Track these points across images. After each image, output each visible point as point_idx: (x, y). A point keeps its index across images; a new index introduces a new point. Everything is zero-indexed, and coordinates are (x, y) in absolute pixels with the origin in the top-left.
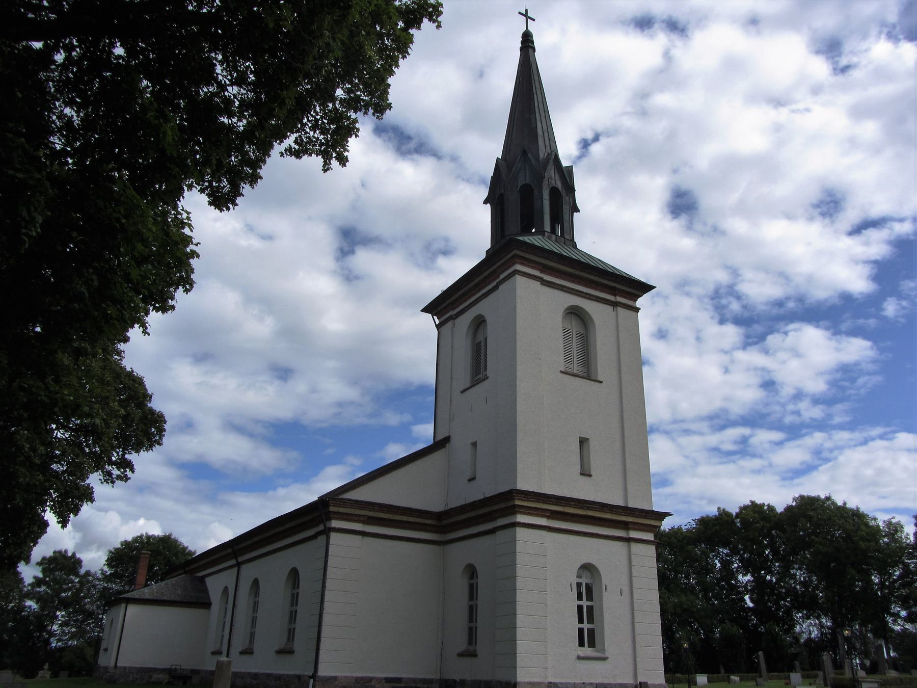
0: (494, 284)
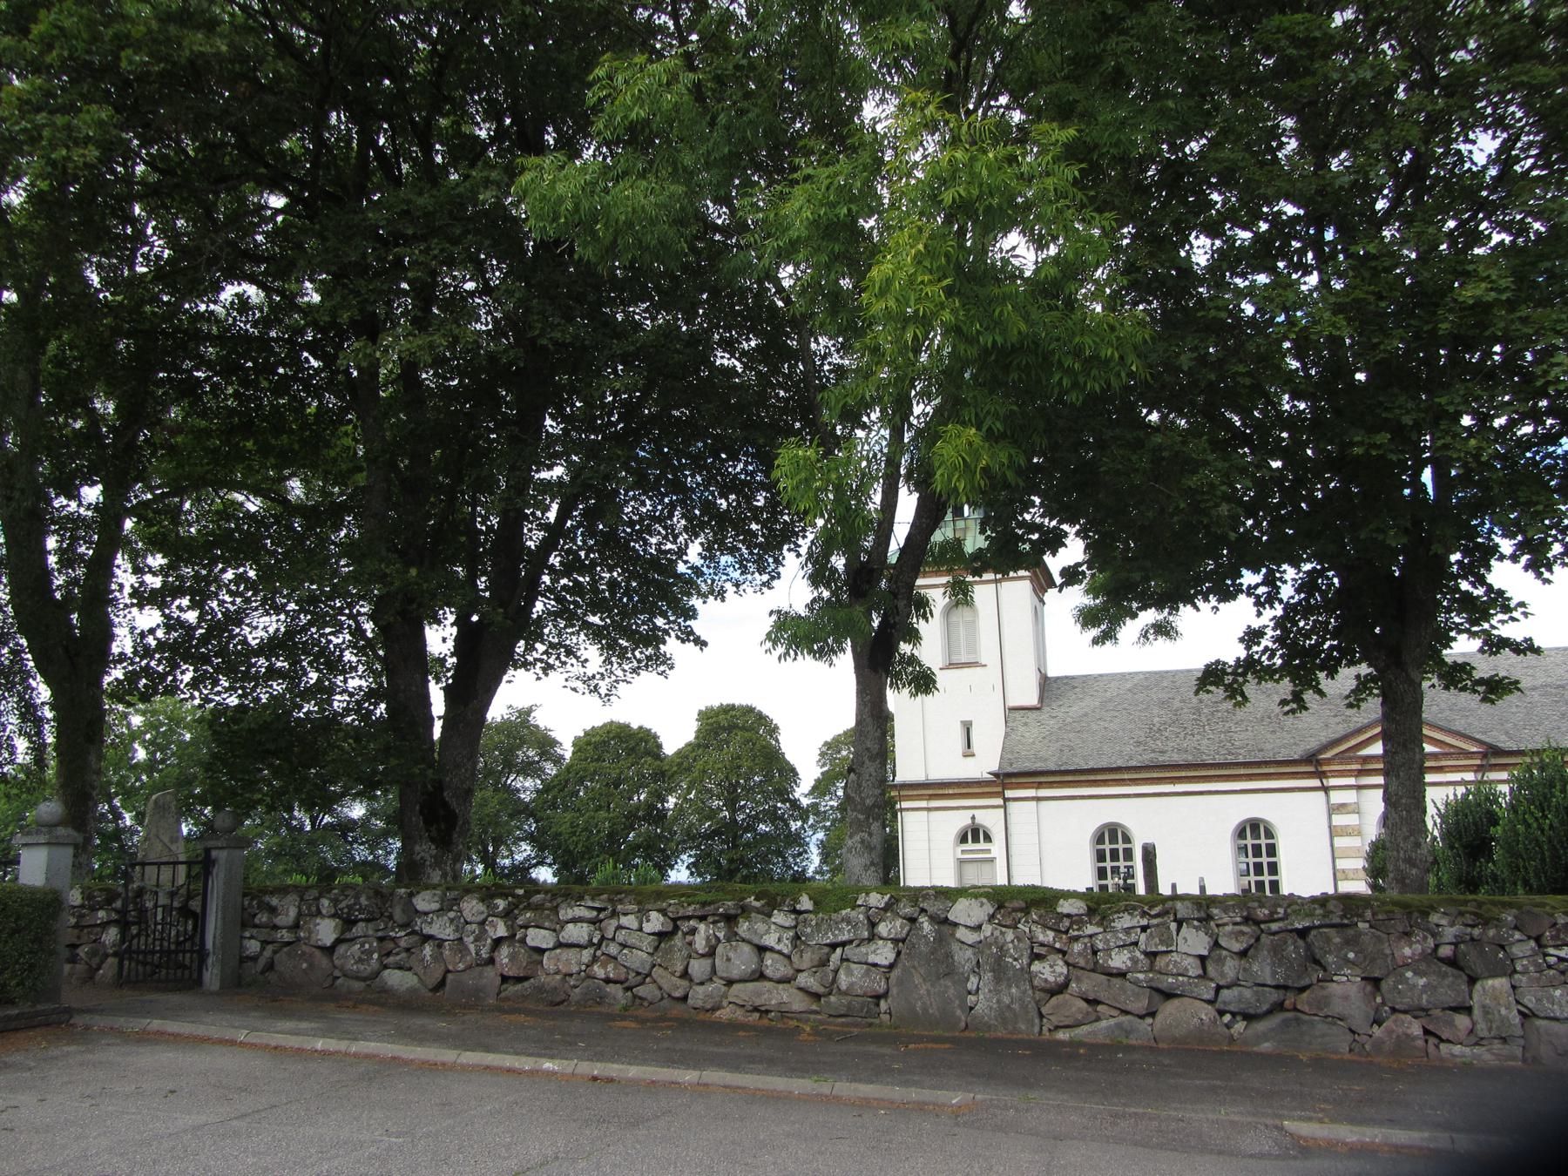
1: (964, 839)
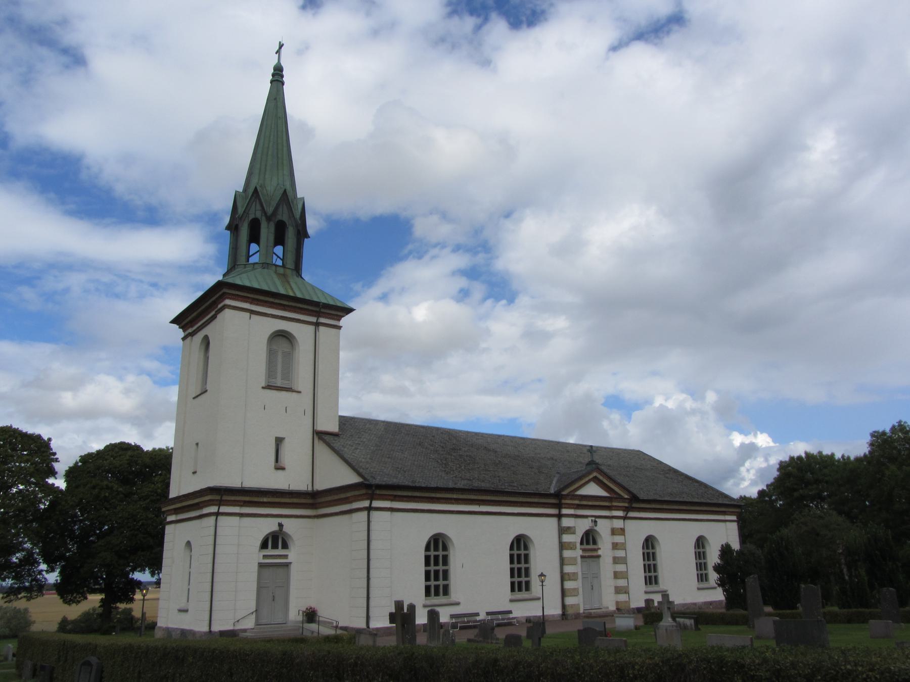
0: (213, 313)
1: (264, 545)
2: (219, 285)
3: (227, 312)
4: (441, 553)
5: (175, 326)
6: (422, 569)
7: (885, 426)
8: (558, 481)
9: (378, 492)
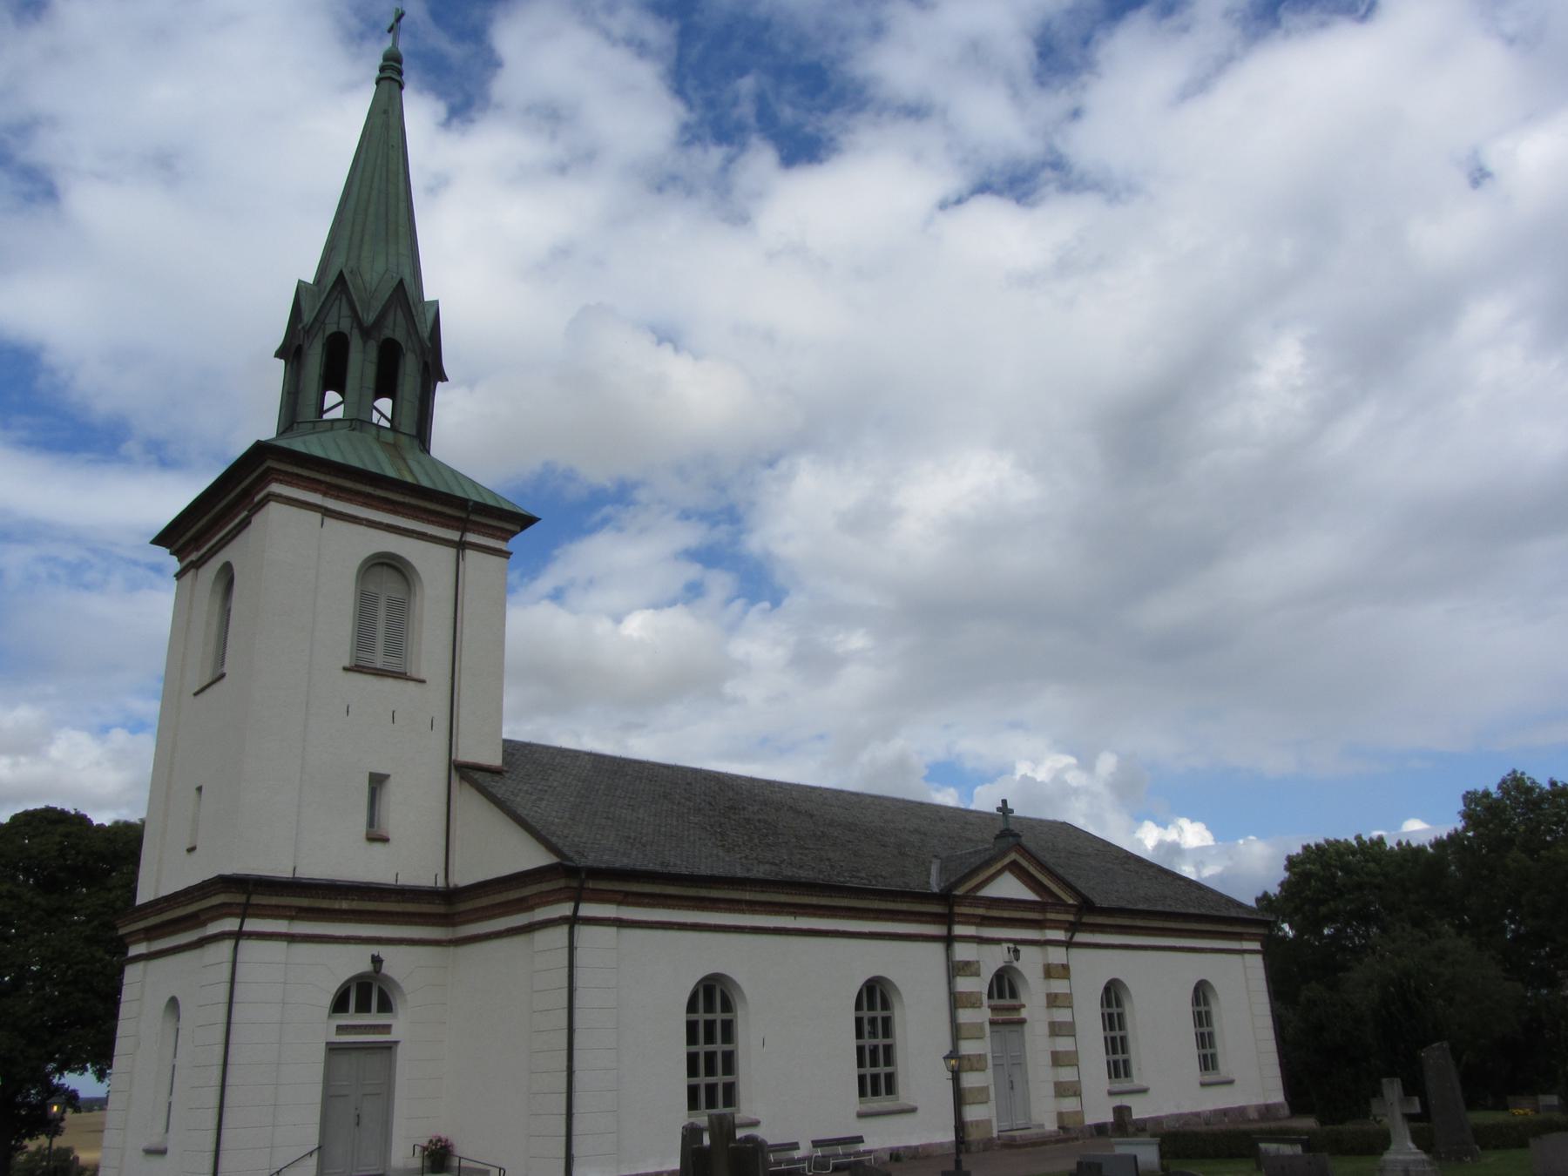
1: (340, 1005)
2: (260, 451)
3: (273, 508)
4: (718, 1016)
5: (163, 555)
6: (681, 1050)
7: (1489, 782)
8: (941, 870)
9: (590, 884)
